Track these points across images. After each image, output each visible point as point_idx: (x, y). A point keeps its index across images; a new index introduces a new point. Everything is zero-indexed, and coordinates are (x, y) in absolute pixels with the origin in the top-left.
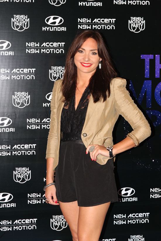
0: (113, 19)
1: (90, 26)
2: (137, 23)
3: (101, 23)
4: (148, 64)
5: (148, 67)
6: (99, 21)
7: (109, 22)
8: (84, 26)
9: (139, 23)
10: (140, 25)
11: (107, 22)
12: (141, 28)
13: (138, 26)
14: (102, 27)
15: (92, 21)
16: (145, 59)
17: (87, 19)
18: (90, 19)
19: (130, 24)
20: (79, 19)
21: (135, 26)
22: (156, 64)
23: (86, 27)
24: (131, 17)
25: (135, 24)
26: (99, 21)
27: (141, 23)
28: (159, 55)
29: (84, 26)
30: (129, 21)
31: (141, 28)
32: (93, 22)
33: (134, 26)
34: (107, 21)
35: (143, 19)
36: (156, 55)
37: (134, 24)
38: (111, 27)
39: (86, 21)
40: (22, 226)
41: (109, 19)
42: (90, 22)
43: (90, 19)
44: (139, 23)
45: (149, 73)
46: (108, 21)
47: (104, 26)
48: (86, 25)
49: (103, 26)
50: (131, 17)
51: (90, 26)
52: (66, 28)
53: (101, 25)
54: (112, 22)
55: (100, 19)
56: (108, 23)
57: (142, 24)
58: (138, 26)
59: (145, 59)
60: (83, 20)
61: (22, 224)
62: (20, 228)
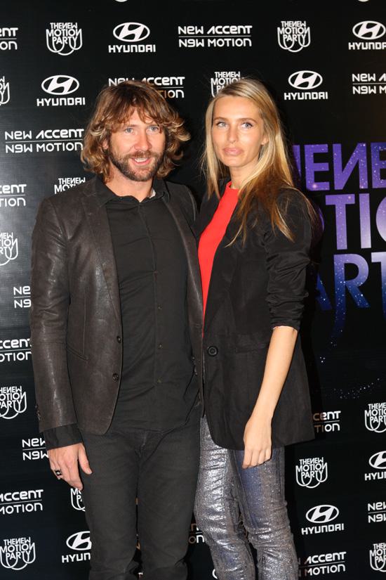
7: (171, 84)
24: (216, 73)
40: (12, 505)
41: (172, 78)
46: (169, 82)
50: (216, 73)
52: (84, 99)
61: (13, 501)
62: (10, 510)
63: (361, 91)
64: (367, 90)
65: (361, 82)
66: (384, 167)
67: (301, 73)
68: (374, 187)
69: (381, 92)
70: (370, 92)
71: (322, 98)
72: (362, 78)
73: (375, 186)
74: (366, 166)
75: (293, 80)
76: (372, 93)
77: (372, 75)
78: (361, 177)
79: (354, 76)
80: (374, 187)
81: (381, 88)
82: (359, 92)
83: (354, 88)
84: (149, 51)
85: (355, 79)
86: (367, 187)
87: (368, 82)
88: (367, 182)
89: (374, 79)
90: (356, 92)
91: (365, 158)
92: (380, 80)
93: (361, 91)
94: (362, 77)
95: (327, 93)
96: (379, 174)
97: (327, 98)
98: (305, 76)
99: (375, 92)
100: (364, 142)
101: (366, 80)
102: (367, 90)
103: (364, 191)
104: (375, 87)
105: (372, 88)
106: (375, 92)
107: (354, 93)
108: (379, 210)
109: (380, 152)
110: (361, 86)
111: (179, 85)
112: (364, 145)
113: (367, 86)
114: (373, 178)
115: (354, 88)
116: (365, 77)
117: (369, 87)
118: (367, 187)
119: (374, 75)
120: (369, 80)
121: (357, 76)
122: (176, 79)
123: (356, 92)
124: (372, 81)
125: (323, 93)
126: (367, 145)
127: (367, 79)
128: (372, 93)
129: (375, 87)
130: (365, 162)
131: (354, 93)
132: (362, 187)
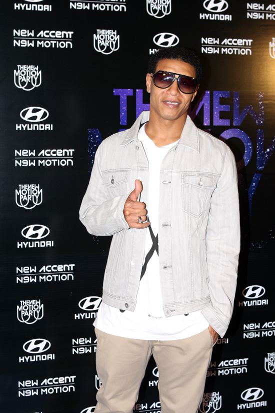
0: (69, 32)
1: (33, 41)
2: (106, 39)
3: (50, 37)
4: (126, 104)
5: (124, 108)
6: (47, 34)
7: (63, 37)
8: (23, 42)
9: (111, 39)
14: (52, 44)
15: (36, 34)
16: (119, 96)
17: (28, 31)
18: (33, 31)
19: (96, 41)
20: (15, 31)
22: (137, 104)
23: (26, 43)
25: (104, 40)
26: (47, 34)
27: (113, 39)
28: (142, 90)
29: (23, 42)
30: (95, 35)
32: (38, 36)
33: (103, 43)
35: (115, 34)
36: (137, 90)
39: (27, 34)
41: (63, 32)
42: (33, 35)
43: (33, 31)
44: (111, 39)
45: (126, 118)
47: (55, 42)
48: (27, 40)
51: (33, 41)
53: (50, 41)
55: (48, 32)
56: (61, 38)
57: (115, 41)
59: (119, 96)
60: (23, 33)
63: (208, 51)
64: (212, 51)
65: (208, 44)
66: (222, 110)
68: (214, 125)
69: (222, 53)
70: (214, 52)
72: (209, 41)
73: (215, 124)
74: (209, 108)
75: (157, 39)
77: (216, 40)
78: (205, 117)
79: (203, 39)
80: (214, 125)
82: (206, 52)
84: (46, 10)
85: (204, 42)
86: (209, 125)
87: (213, 44)
88: (209, 120)
89: (218, 43)
90: (204, 51)
91: (209, 102)
92: (222, 43)
93: (208, 51)
94: (209, 40)
96: (219, 115)
98: (166, 37)
99: (218, 52)
101: (212, 43)
102: (212, 50)
104: (218, 49)
105: (216, 49)
106: (218, 52)
109: (220, 98)
110: (208, 47)
111: (69, 38)
112: (208, 92)
113: (213, 47)
114: (214, 118)
116: (211, 41)
117: (214, 48)
118: (209, 125)
119: (218, 39)
120: (214, 43)
121: (205, 39)
122: (67, 33)
123: (204, 51)
124: (216, 43)
126: (210, 92)
127: (213, 42)
128: (216, 53)
129: (218, 49)
130: (209, 105)
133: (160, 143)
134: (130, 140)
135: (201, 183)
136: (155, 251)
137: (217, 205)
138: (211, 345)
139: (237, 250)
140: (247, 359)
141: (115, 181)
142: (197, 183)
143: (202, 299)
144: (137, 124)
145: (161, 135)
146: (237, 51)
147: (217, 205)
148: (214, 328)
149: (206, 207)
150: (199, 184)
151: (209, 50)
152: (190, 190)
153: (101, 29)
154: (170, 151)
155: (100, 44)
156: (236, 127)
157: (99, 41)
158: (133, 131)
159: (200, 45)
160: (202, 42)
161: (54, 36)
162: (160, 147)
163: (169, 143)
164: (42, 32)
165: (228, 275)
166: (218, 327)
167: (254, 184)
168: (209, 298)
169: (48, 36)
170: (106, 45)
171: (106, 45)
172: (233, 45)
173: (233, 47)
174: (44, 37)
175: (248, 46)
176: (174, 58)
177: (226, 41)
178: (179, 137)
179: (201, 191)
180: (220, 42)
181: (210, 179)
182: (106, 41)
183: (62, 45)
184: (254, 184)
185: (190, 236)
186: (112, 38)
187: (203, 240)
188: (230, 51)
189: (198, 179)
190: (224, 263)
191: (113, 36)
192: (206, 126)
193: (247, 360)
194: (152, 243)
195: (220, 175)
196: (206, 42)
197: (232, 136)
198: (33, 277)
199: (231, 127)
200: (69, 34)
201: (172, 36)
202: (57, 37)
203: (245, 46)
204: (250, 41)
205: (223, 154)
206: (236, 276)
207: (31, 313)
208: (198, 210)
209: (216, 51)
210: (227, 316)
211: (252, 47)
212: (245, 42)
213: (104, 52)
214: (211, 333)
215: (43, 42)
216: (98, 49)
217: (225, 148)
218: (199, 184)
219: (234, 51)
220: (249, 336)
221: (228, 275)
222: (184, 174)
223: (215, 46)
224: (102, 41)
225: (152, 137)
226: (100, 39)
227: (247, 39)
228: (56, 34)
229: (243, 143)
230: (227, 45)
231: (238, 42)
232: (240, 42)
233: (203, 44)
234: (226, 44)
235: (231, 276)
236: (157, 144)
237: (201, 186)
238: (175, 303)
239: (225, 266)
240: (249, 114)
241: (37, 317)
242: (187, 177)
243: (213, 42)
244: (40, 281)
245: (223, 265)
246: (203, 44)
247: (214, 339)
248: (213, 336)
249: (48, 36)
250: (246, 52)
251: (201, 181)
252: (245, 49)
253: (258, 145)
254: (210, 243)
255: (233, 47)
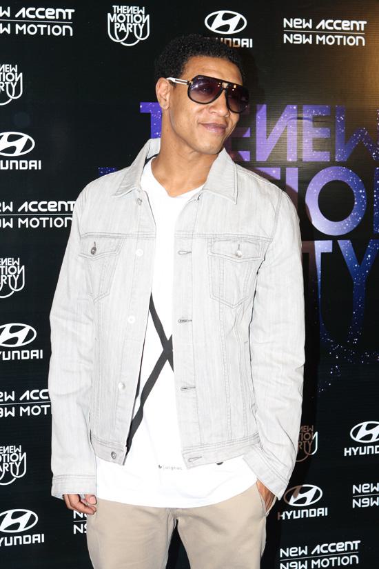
0: (67, 10)
1: (9, 25)
2: (128, 21)
7: (57, 17)
10: (137, 26)
11: (53, 17)
12: (139, 35)
13: (133, 29)
14: (39, 29)
15: (13, 13)
19: (112, 24)
21: (124, 29)
24: (115, 7)
25: (125, 23)
27: (140, 21)
30: (109, 15)
31: (139, 35)
32: (17, 16)
33: (122, 28)
34: (53, 13)
35: (143, 12)
37: (123, 25)
38: (62, 31)
41: (58, 10)
43: (9, 8)
47: (45, 26)
49: (42, 27)
51: (9, 25)
53: (36, 24)
54: (64, 17)
55: (33, 9)
56: (55, 20)
57: (143, 25)
58: (133, 29)
63: (294, 40)
64: (301, 39)
65: (293, 28)
66: (317, 136)
67: (221, 13)
69: (317, 43)
70: (304, 42)
71: (245, 46)
72: (295, 23)
75: (211, 22)
76: (307, 42)
77: (307, 21)
81: (318, 37)
82: (291, 41)
83: (285, 36)
85: (287, 24)
87: (302, 29)
89: (310, 27)
90: (287, 40)
92: (318, 27)
93: (294, 40)
94: (294, 23)
95: (251, 40)
97: (251, 46)
98: (226, 17)
99: (310, 42)
100: (293, 104)
101: (300, 27)
102: (300, 39)
103: (291, 165)
105: (307, 37)
106: (310, 42)
107: (285, 42)
108: (311, 184)
110: (294, 33)
112: (295, 108)
113: (302, 34)
115: (285, 36)
116: (300, 23)
120: (304, 26)
122: (64, 12)
123: (287, 40)
124: (307, 28)
125: (247, 40)
126: (298, 109)
127: (302, 25)
128: (307, 42)
131: (285, 42)
132: (290, 160)
133: (174, 191)
134: (128, 188)
135: (240, 253)
136: (167, 363)
137: (267, 287)
138: (263, 512)
139: (301, 359)
140: (359, 542)
141: (97, 252)
142: (234, 253)
143: (246, 438)
144: (139, 162)
145: (177, 179)
146: (342, 40)
147: (267, 287)
148: (266, 483)
149: (248, 290)
150: (237, 255)
151: (296, 39)
152: (222, 264)
153: (120, 5)
154: (190, 202)
155: (118, 29)
156: (340, 164)
157: (116, 24)
158: (134, 172)
159: (281, 30)
160: (285, 26)
161: (43, 17)
162: (173, 197)
163: (189, 190)
164: (23, 10)
165: (286, 398)
166: (272, 482)
167: (369, 256)
168: (256, 436)
169: (33, 17)
170: (128, 30)
171: (128, 30)
172: (334, 30)
173: (334, 32)
174: (27, 18)
175: (360, 31)
176: (208, 54)
177: (323, 24)
178: (203, 181)
179: (239, 266)
180: (314, 25)
181: (255, 246)
182: (128, 25)
183: (57, 30)
184: (369, 256)
185: (223, 338)
186: (138, 19)
187: (245, 343)
188: (330, 40)
189: (235, 246)
190: (279, 380)
191: (140, 16)
192: (289, 162)
193: (358, 544)
194: (161, 350)
195: (270, 240)
196: (291, 26)
197: (334, 178)
198: (10, 409)
199: (332, 163)
200: (67, 13)
201: (235, 15)
202: (48, 17)
203: (354, 32)
204: (363, 23)
205: (275, 207)
206: (300, 399)
207: (6, 468)
208: (236, 296)
209: (307, 39)
210: (286, 464)
211: (367, 32)
212: (355, 25)
213: (124, 42)
214: (260, 491)
215: (24, 26)
216: (116, 39)
217: (280, 197)
218: (237, 255)
219: (336, 39)
220: (362, 504)
221: (286, 398)
222: (213, 239)
223: (306, 32)
224: (121, 24)
225: (162, 181)
226: (117, 22)
227: (358, 21)
228: (47, 13)
229: (351, 190)
230: (326, 29)
231: (343, 25)
232: (346, 25)
233: (285, 29)
234: (323, 28)
235: (291, 400)
236: (171, 193)
237: (240, 257)
238: (202, 445)
239: (281, 384)
240: (361, 143)
241: (15, 474)
242: (217, 244)
243: (302, 25)
244: (21, 415)
245: (277, 382)
246: (285, 29)
247: (266, 501)
248: (264, 495)
249: (33, 17)
250: (356, 41)
251: (239, 249)
252: (355, 36)
253: (375, 194)
254: (254, 347)
255: (334, 32)
